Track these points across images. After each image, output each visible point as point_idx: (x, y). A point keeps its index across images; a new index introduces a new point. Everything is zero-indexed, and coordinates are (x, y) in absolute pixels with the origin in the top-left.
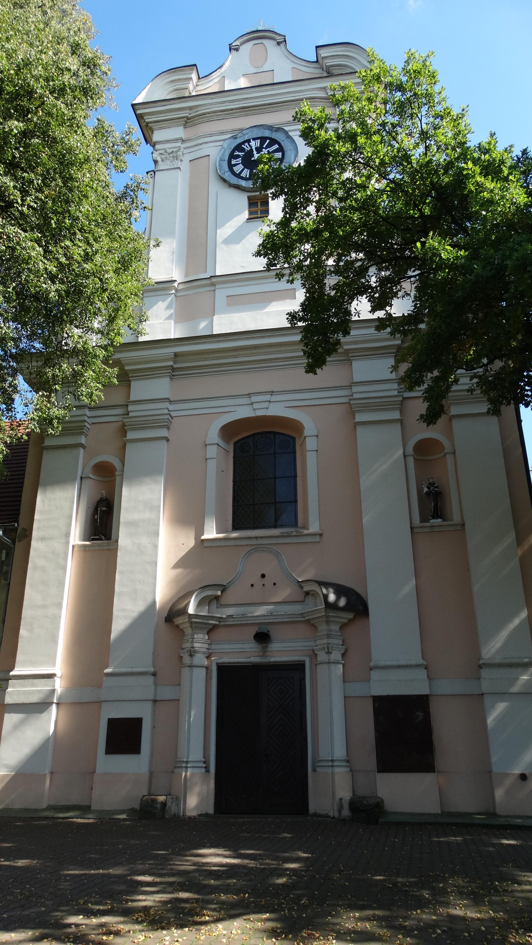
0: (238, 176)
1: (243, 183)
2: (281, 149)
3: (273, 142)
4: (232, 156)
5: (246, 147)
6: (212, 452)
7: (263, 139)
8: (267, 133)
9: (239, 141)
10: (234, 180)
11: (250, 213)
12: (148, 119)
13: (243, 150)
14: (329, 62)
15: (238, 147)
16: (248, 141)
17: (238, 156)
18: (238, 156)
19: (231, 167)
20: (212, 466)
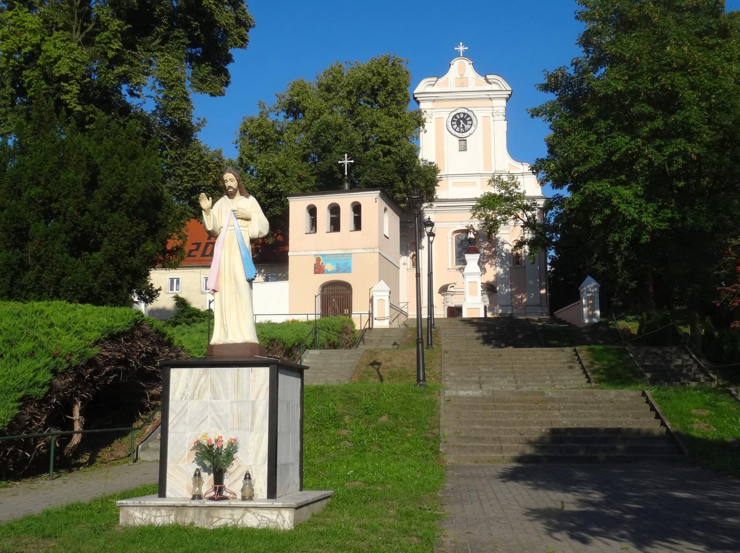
0: (455, 130)
1: (457, 134)
2: (471, 120)
3: (468, 116)
4: (452, 121)
5: (458, 116)
6: (450, 240)
7: (464, 114)
8: (466, 111)
9: (455, 113)
10: (454, 132)
11: (460, 146)
12: (419, 99)
13: (456, 118)
14: (490, 81)
15: (455, 116)
16: (459, 114)
17: (454, 121)
18: (454, 121)
19: (452, 125)
20: (450, 245)
